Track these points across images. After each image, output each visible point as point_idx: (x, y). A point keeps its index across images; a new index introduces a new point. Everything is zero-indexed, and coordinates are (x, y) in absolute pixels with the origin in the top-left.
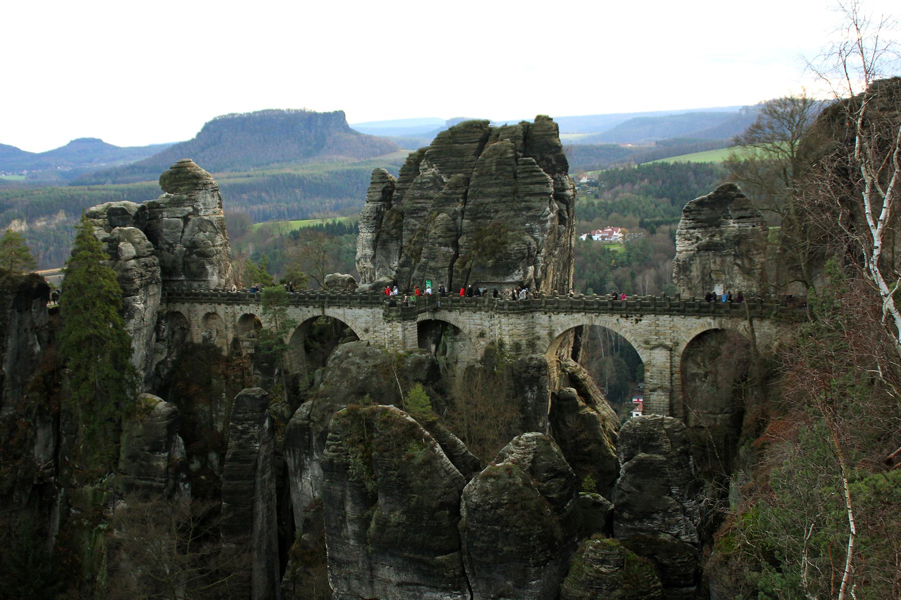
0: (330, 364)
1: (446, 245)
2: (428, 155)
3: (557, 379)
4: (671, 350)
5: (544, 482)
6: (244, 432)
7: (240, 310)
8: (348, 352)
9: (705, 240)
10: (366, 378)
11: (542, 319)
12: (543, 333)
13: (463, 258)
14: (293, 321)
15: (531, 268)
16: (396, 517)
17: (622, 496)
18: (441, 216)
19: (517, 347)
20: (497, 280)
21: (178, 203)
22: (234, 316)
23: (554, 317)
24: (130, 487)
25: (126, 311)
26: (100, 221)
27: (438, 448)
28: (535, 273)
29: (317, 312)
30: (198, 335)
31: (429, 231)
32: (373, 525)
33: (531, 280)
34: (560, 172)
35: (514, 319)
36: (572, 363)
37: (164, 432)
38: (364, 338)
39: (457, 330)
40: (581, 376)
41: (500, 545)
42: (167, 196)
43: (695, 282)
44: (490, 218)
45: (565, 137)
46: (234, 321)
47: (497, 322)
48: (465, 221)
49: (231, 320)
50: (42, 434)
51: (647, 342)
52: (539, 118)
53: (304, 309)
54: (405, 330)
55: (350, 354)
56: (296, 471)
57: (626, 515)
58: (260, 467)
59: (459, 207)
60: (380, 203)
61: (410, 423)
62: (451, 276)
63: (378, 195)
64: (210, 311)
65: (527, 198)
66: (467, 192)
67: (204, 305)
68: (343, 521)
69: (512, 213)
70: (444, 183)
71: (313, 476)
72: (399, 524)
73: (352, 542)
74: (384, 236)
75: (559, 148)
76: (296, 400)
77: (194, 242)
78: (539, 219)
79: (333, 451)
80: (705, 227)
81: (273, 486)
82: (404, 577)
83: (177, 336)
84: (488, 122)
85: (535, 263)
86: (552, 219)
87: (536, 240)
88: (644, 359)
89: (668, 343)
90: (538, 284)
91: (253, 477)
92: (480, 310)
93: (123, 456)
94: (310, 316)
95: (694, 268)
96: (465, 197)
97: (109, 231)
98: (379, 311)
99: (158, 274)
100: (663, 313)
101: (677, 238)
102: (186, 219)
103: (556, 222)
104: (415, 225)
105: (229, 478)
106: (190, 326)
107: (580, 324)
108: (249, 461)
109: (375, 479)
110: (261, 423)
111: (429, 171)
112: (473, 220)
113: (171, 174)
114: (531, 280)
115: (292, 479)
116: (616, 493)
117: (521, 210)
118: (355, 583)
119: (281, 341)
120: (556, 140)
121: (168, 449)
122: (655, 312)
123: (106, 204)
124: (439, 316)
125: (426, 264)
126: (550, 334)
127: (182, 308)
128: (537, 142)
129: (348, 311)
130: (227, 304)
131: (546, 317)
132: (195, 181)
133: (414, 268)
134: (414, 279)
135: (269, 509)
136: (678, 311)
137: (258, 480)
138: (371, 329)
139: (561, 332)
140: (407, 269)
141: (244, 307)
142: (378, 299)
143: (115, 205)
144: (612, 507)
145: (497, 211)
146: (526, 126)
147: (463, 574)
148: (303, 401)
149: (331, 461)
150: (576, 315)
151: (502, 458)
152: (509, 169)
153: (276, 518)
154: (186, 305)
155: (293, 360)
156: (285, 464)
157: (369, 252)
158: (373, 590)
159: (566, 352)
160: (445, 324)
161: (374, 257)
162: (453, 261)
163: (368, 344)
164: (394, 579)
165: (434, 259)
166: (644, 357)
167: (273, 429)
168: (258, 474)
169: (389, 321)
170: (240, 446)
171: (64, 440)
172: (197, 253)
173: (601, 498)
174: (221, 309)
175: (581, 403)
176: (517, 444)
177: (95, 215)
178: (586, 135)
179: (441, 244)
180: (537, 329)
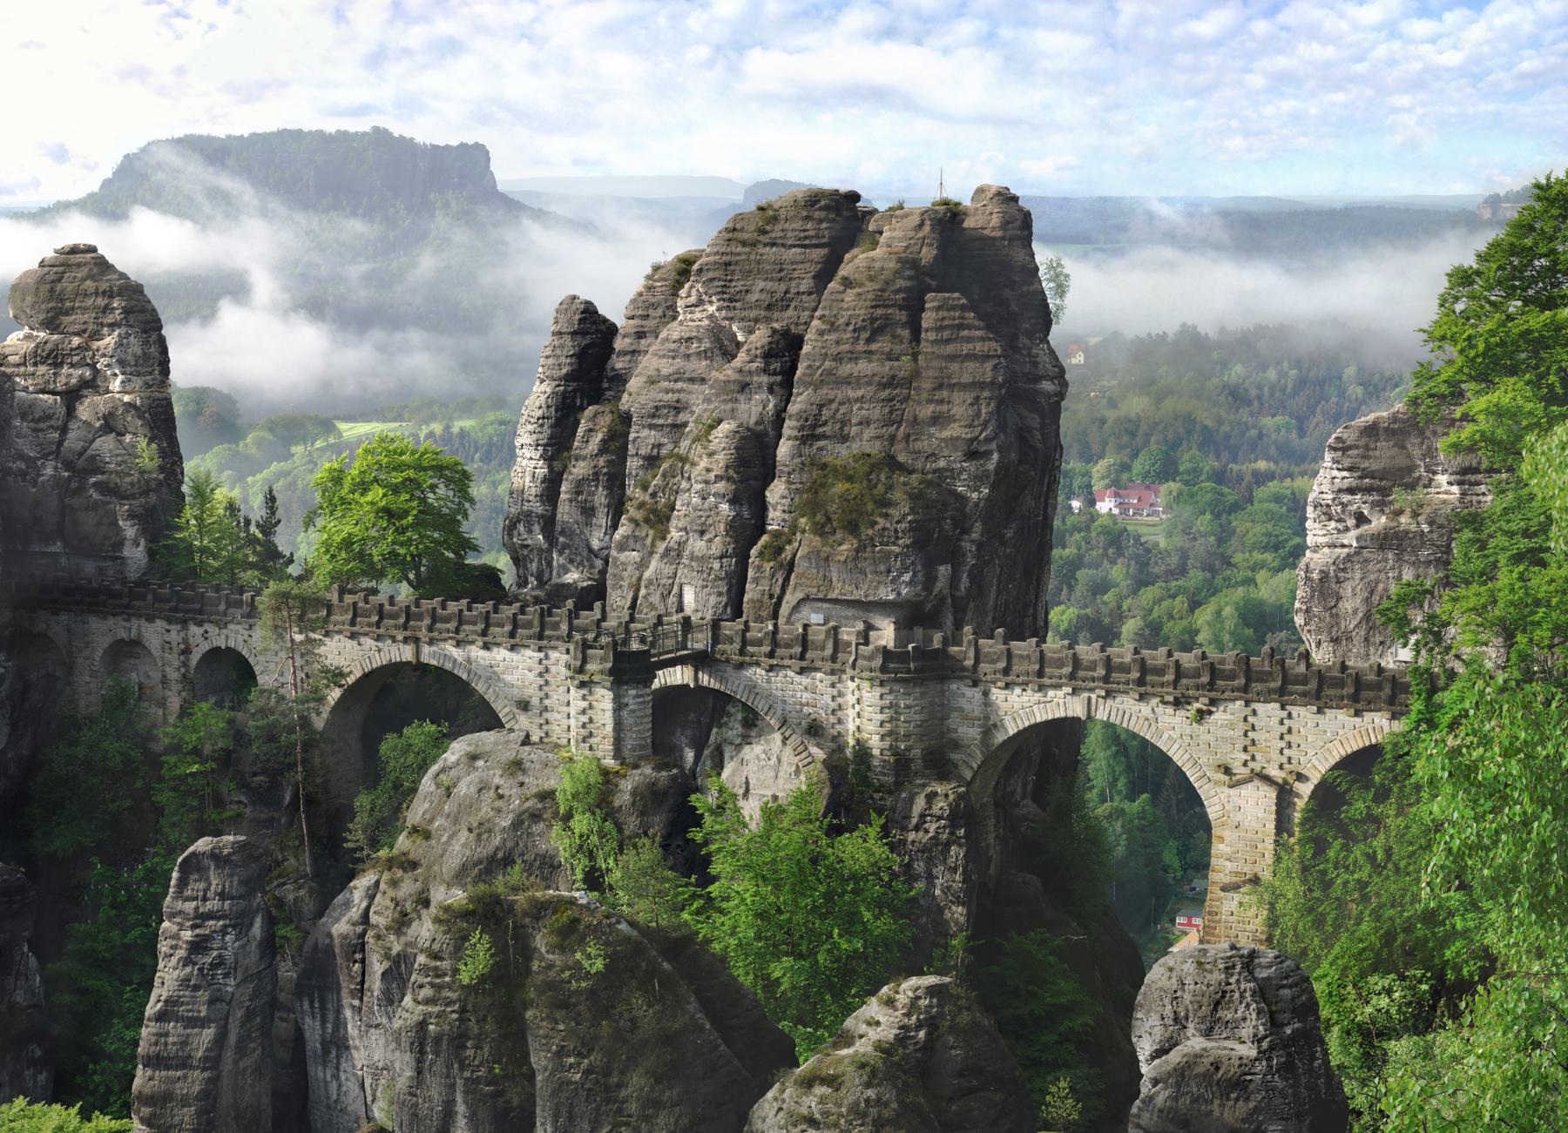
2: (700, 271)
5: (951, 1100)
8: (474, 757)
9: (1379, 522)
10: (517, 824)
12: (969, 733)
13: (776, 534)
14: (337, 675)
15: (944, 570)
18: (725, 427)
20: (858, 595)
22: (187, 651)
28: (954, 580)
31: (693, 464)
33: (942, 600)
34: (1030, 335)
42: (28, 337)
44: (844, 438)
46: (185, 664)
47: (851, 699)
49: (174, 659)
52: (980, 191)
53: (368, 642)
54: (619, 707)
55: (480, 763)
56: (326, 1052)
58: (232, 1039)
60: (572, 386)
61: (628, 939)
64: (123, 635)
65: (945, 393)
66: (793, 368)
67: (111, 621)
70: (739, 345)
74: (579, 469)
76: (335, 871)
77: (93, 457)
79: (427, 1002)
80: (1379, 490)
84: (854, 197)
88: (1213, 812)
89: (1274, 772)
90: (960, 610)
94: (379, 661)
95: (1347, 590)
98: (559, 659)
101: (1310, 512)
104: (660, 446)
106: (70, 669)
107: (1060, 714)
108: (202, 1023)
110: (240, 923)
113: (42, 280)
114: (942, 600)
115: (317, 1072)
120: (1020, 256)
122: (1246, 694)
130: (170, 621)
131: (974, 694)
132: (101, 301)
133: (651, 553)
134: (650, 583)
136: (1304, 694)
137: (227, 1066)
138: (535, 701)
139: (1012, 730)
140: (635, 556)
141: (212, 629)
142: (556, 626)
145: (865, 423)
146: (948, 218)
148: (352, 875)
151: (847, 1039)
152: (902, 316)
154: (64, 617)
156: (299, 1035)
163: (526, 741)
165: (702, 533)
166: (1216, 800)
167: (270, 947)
168: (229, 1055)
169: (582, 685)
172: (103, 488)
174: (155, 633)
176: (890, 1003)
180: (953, 721)
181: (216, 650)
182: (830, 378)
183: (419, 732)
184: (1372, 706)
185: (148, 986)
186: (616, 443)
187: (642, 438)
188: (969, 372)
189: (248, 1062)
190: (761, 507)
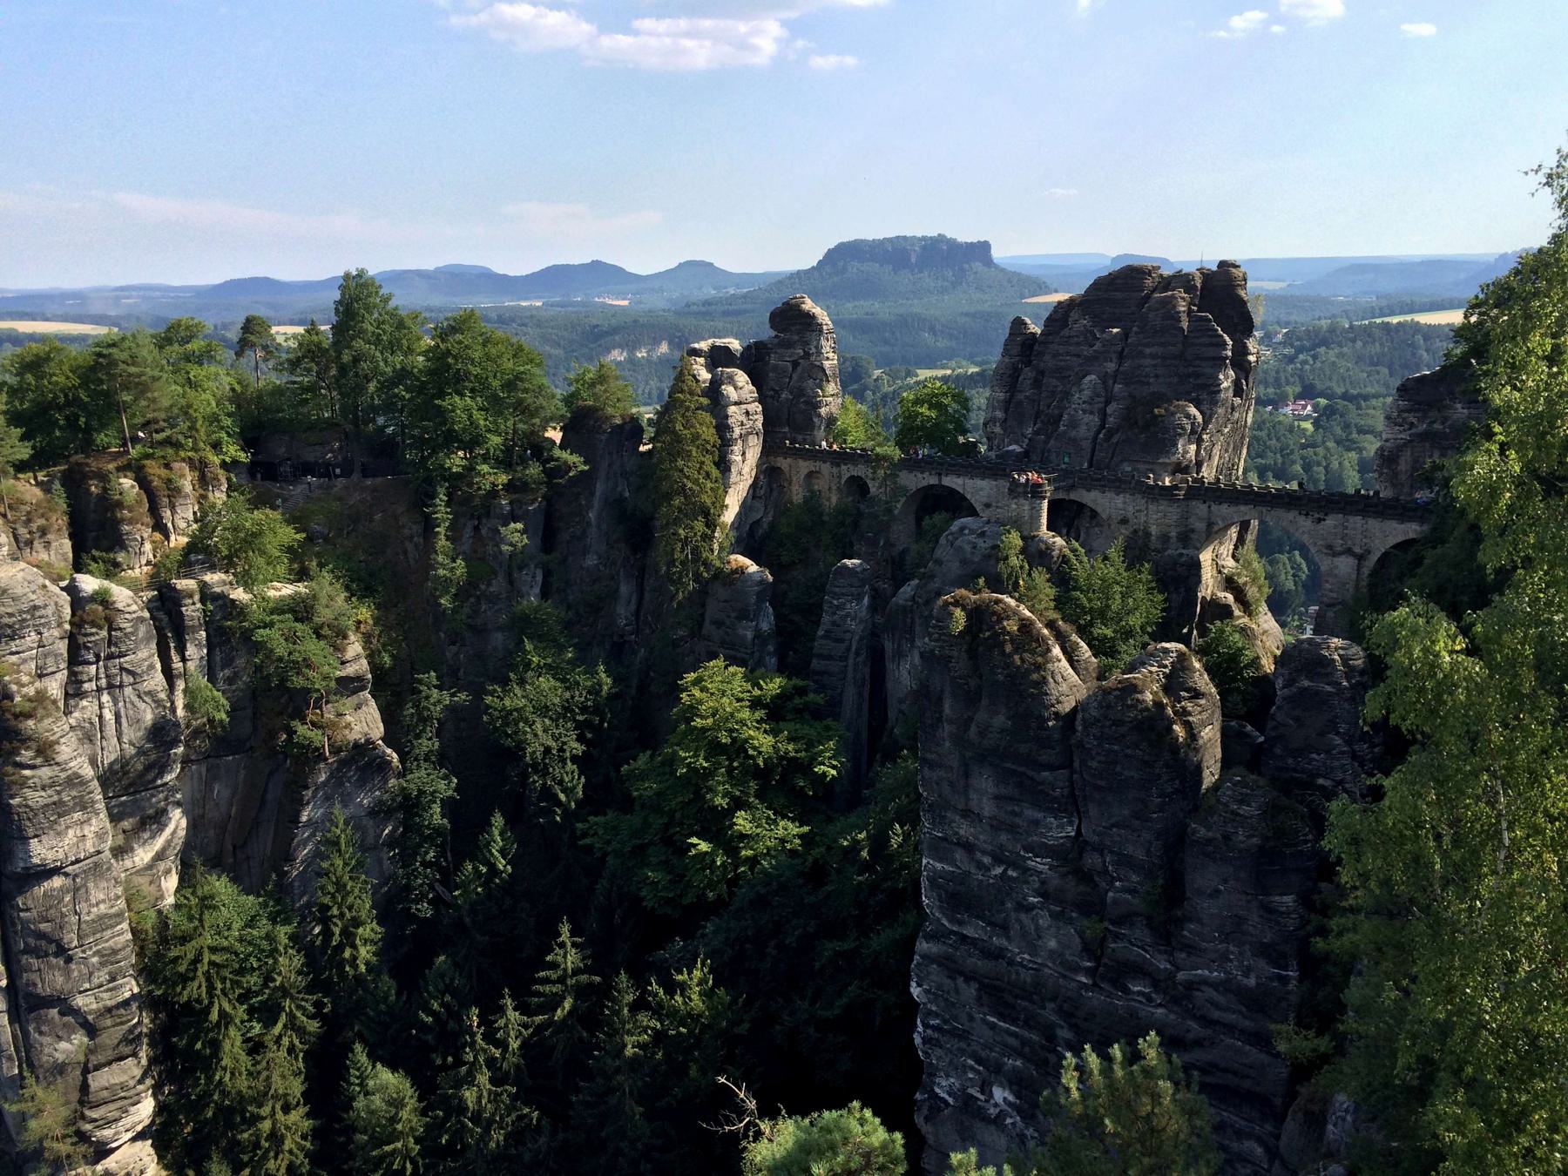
0: (942, 540)
1: (1092, 413)
3: (1211, 582)
4: (1361, 558)
6: (838, 607)
7: (847, 471)
8: (962, 529)
11: (1200, 508)
13: (1109, 430)
14: (905, 489)
16: (1000, 721)
17: (1275, 728)
19: (1165, 538)
20: (1149, 459)
21: (788, 345)
22: (840, 477)
23: (1214, 507)
24: (714, 656)
25: (724, 465)
26: (701, 360)
27: (1057, 651)
28: (1198, 452)
29: (933, 480)
30: (797, 494)
32: (973, 728)
35: (1163, 505)
36: (1230, 563)
37: (753, 599)
38: (985, 515)
39: (1094, 514)
40: (1241, 581)
41: (1118, 769)
43: (1403, 478)
45: (1255, 288)
48: (1118, 387)
50: (624, 589)
51: (1330, 547)
57: (1278, 751)
59: (1111, 366)
61: (1028, 619)
62: (1093, 450)
63: (1016, 350)
68: (940, 720)
69: (1176, 380)
71: (913, 665)
72: (1003, 731)
73: (947, 744)
74: (1020, 397)
75: (1243, 303)
78: (1213, 389)
81: (867, 670)
82: (1003, 791)
83: (775, 494)
85: (1199, 442)
86: (1227, 389)
87: (1202, 413)
89: (1357, 550)
90: (1199, 464)
91: (846, 659)
92: (1124, 491)
93: (707, 623)
94: (925, 483)
95: (1402, 461)
96: (1121, 357)
97: (709, 371)
99: (759, 425)
100: (1351, 513)
102: (795, 364)
103: (1231, 393)
105: (821, 656)
108: (841, 641)
109: (980, 677)
110: (859, 598)
111: (1081, 323)
112: (1127, 384)
115: (890, 666)
116: (1271, 724)
117: (1189, 376)
118: (946, 789)
119: (889, 511)
120: (1242, 293)
121: (756, 617)
122: (1342, 511)
123: (710, 341)
124: (1073, 496)
125: (1065, 432)
126: (1210, 525)
127: (784, 463)
128: (1220, 290)
129: (969, 482)
133: (1049, 437)
135: (860, 695)
137: (851, 661)
143: (719, 342)
144: (1262, 739)
146: (1207, 276)
147: (1072, 794)
149: (932, 651)
150: (1243, 508)
153: (866, 706)
154: (789, 460)
155: (901, 533)
157: (999, 414)
158: (968, 799)
159: (1226, 549)
160: (1082, 506)
161: (1005, 421)
162: (1098, 432)
164: (992, 790)
166: (1325, 564)
167: (873, 608)
168: (852, 656)
170: (834, 623)
171: (647, 596)
172: (806, 403)
173: (1249, 728)
174: (826, 468)
175: (1237, 613)
177: (696, 353)
178: (1283, 285)
179: (1084, 411)
181: (852, 477)
182: (1141, 355)
183: (938, 518)
184: (1410, 519)
185: (817, 623)
186: (1037, 383)
187: (1051, 381)
188: (1211, 352)
189: (860, 659)
190: (1104, 416)
